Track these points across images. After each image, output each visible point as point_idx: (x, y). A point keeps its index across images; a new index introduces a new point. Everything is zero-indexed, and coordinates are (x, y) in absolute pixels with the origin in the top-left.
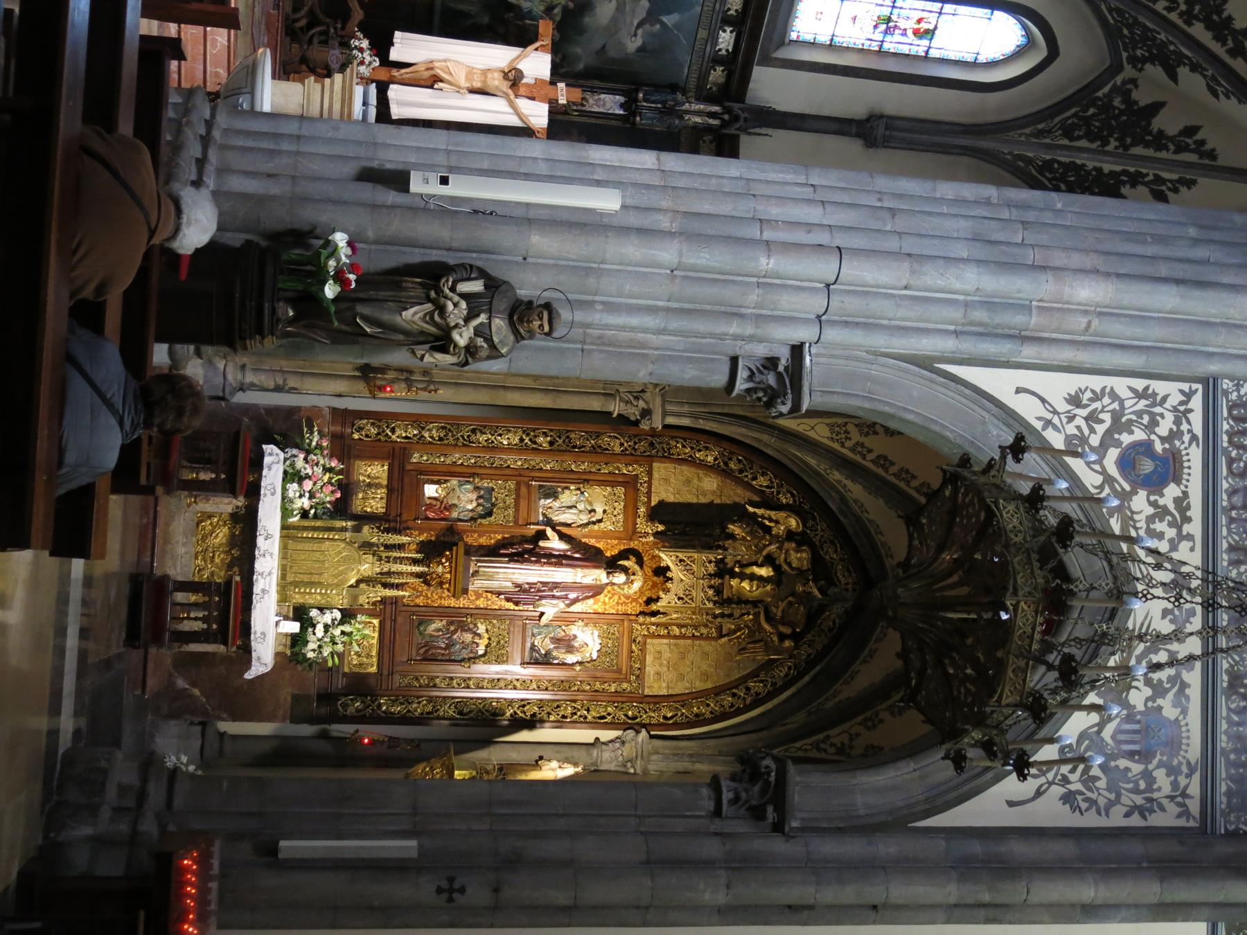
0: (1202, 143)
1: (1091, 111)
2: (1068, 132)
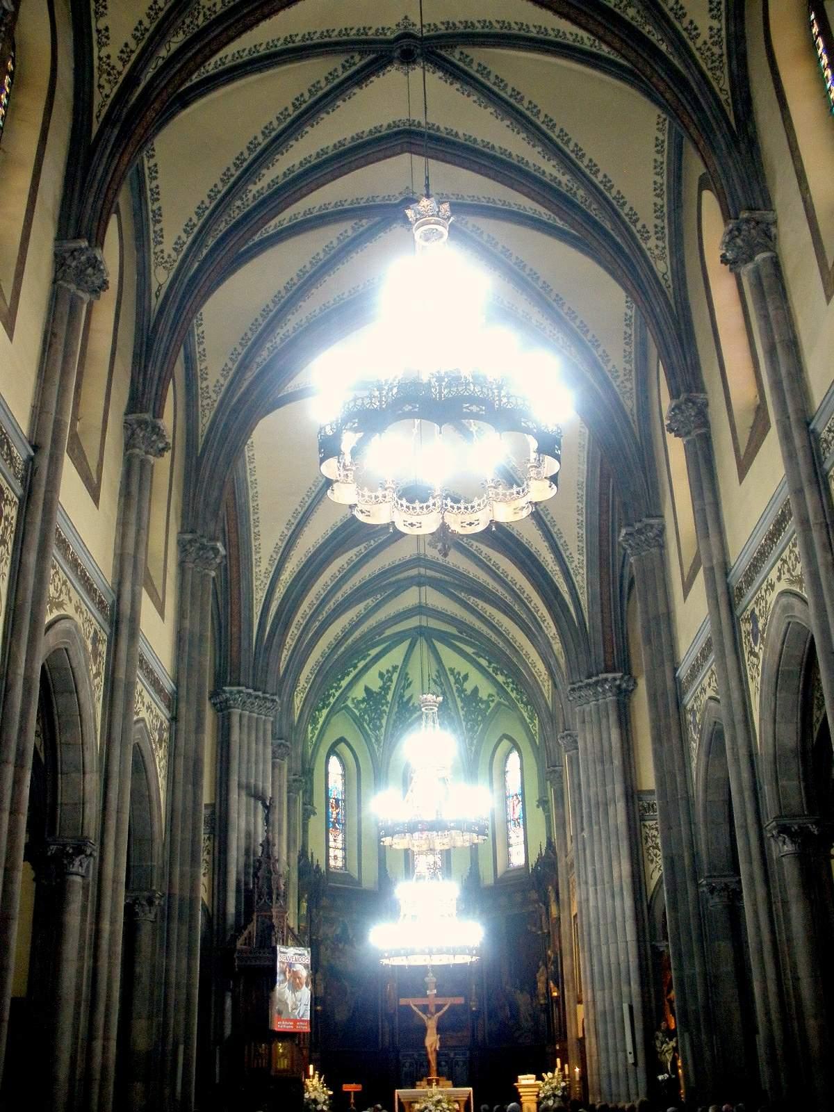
0: (388, 671)
1: (366, 717)
2: (379, 728)
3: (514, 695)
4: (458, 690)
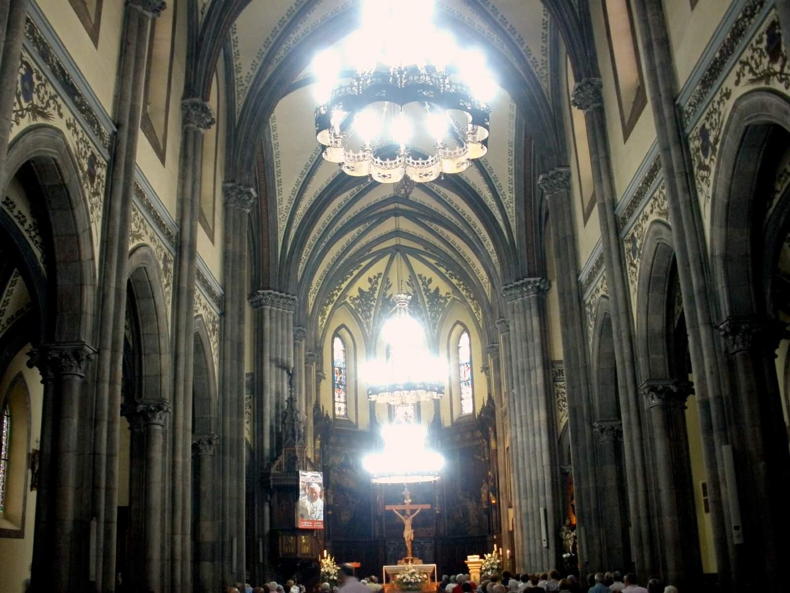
0: (375, 277)
1: (360, 310)
2: (369, 317)
3: (464, 293)
4: (424, 290)
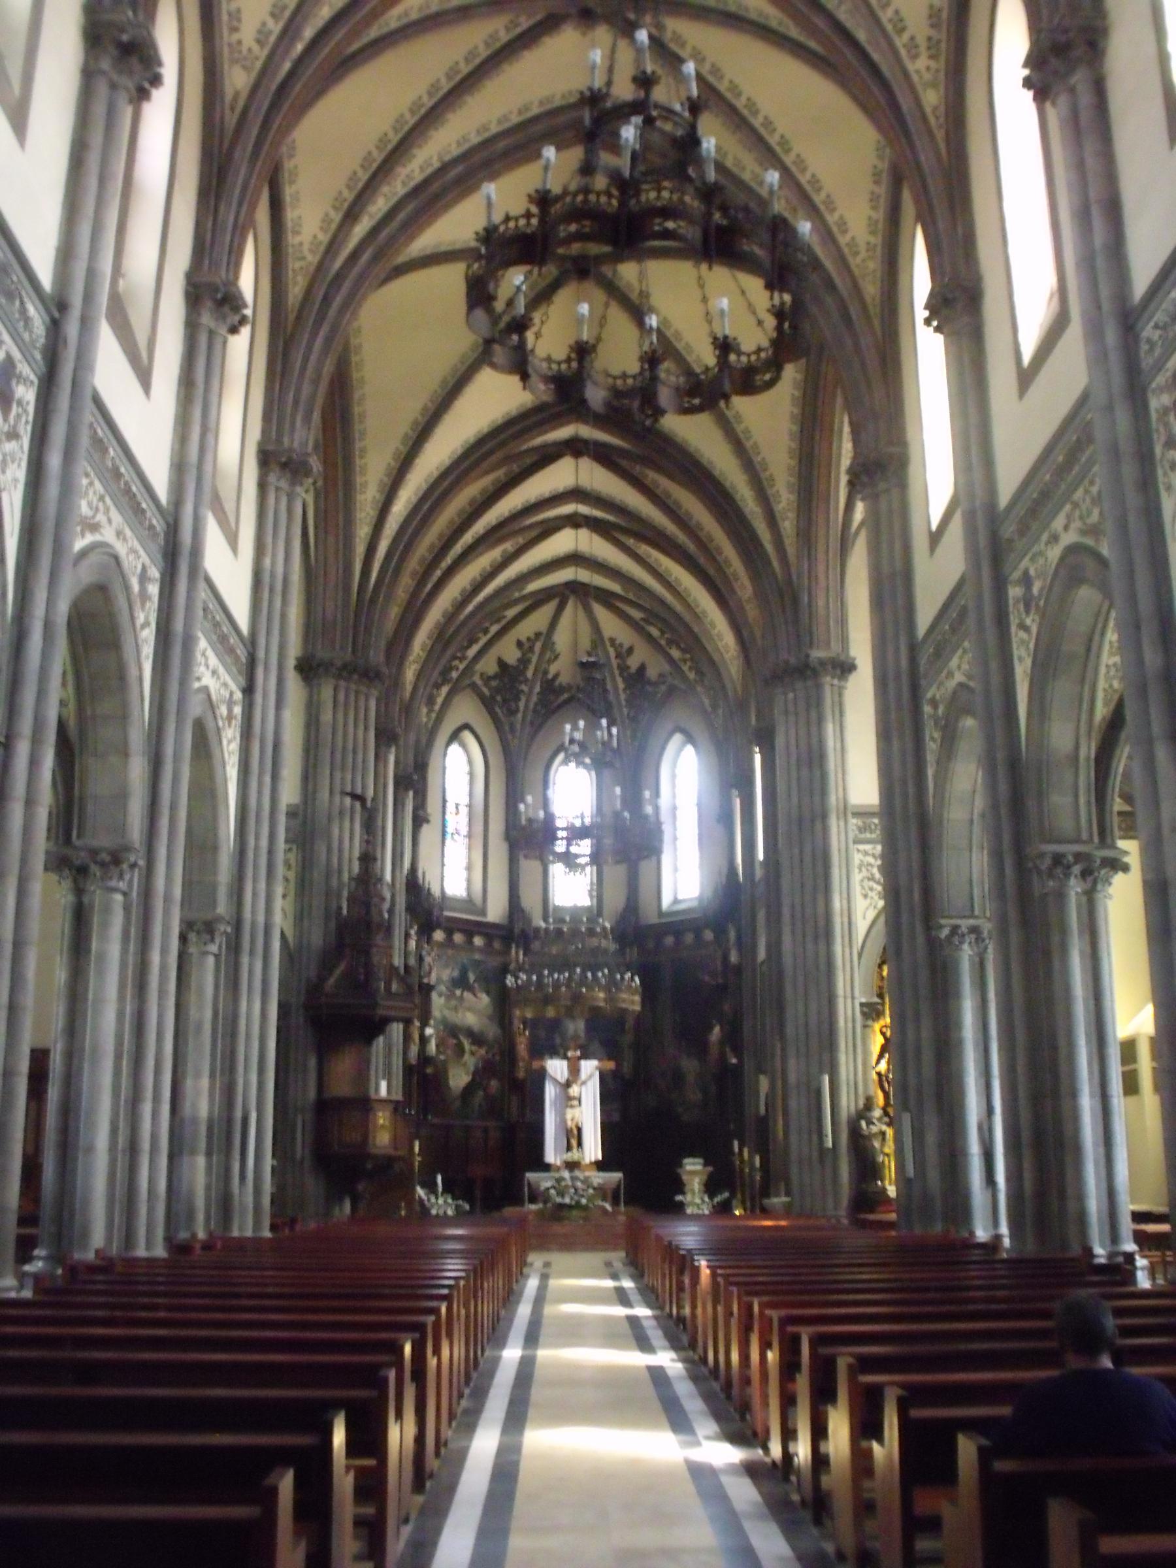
1: (499, 698)
2: (512, 712)
4: (619, 666)
